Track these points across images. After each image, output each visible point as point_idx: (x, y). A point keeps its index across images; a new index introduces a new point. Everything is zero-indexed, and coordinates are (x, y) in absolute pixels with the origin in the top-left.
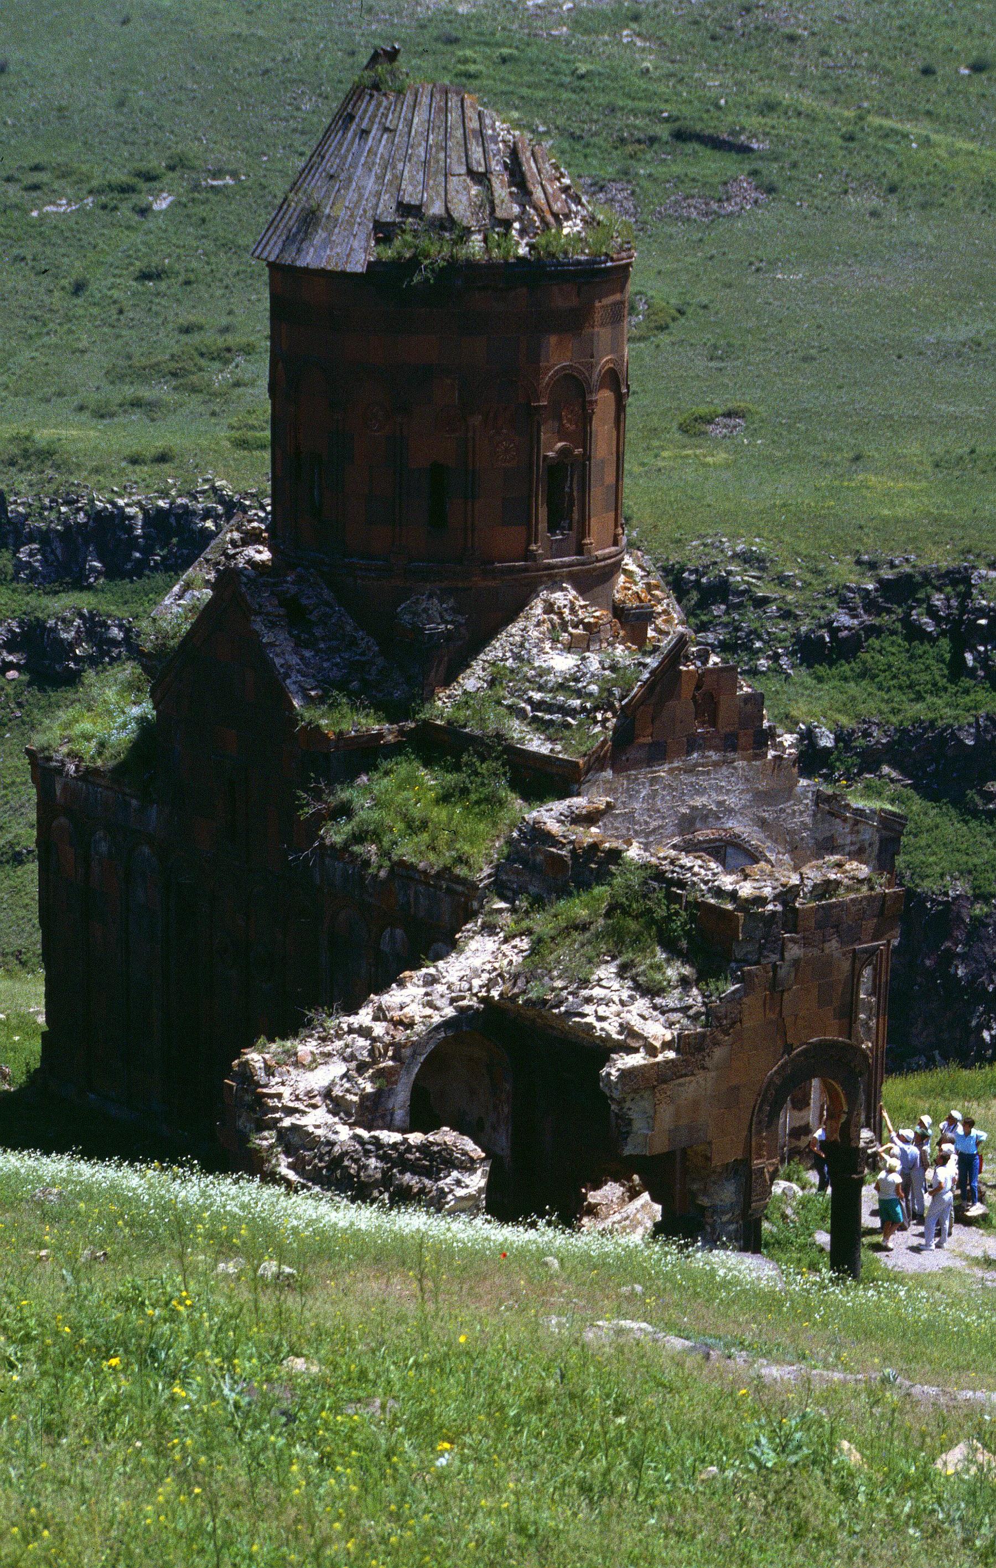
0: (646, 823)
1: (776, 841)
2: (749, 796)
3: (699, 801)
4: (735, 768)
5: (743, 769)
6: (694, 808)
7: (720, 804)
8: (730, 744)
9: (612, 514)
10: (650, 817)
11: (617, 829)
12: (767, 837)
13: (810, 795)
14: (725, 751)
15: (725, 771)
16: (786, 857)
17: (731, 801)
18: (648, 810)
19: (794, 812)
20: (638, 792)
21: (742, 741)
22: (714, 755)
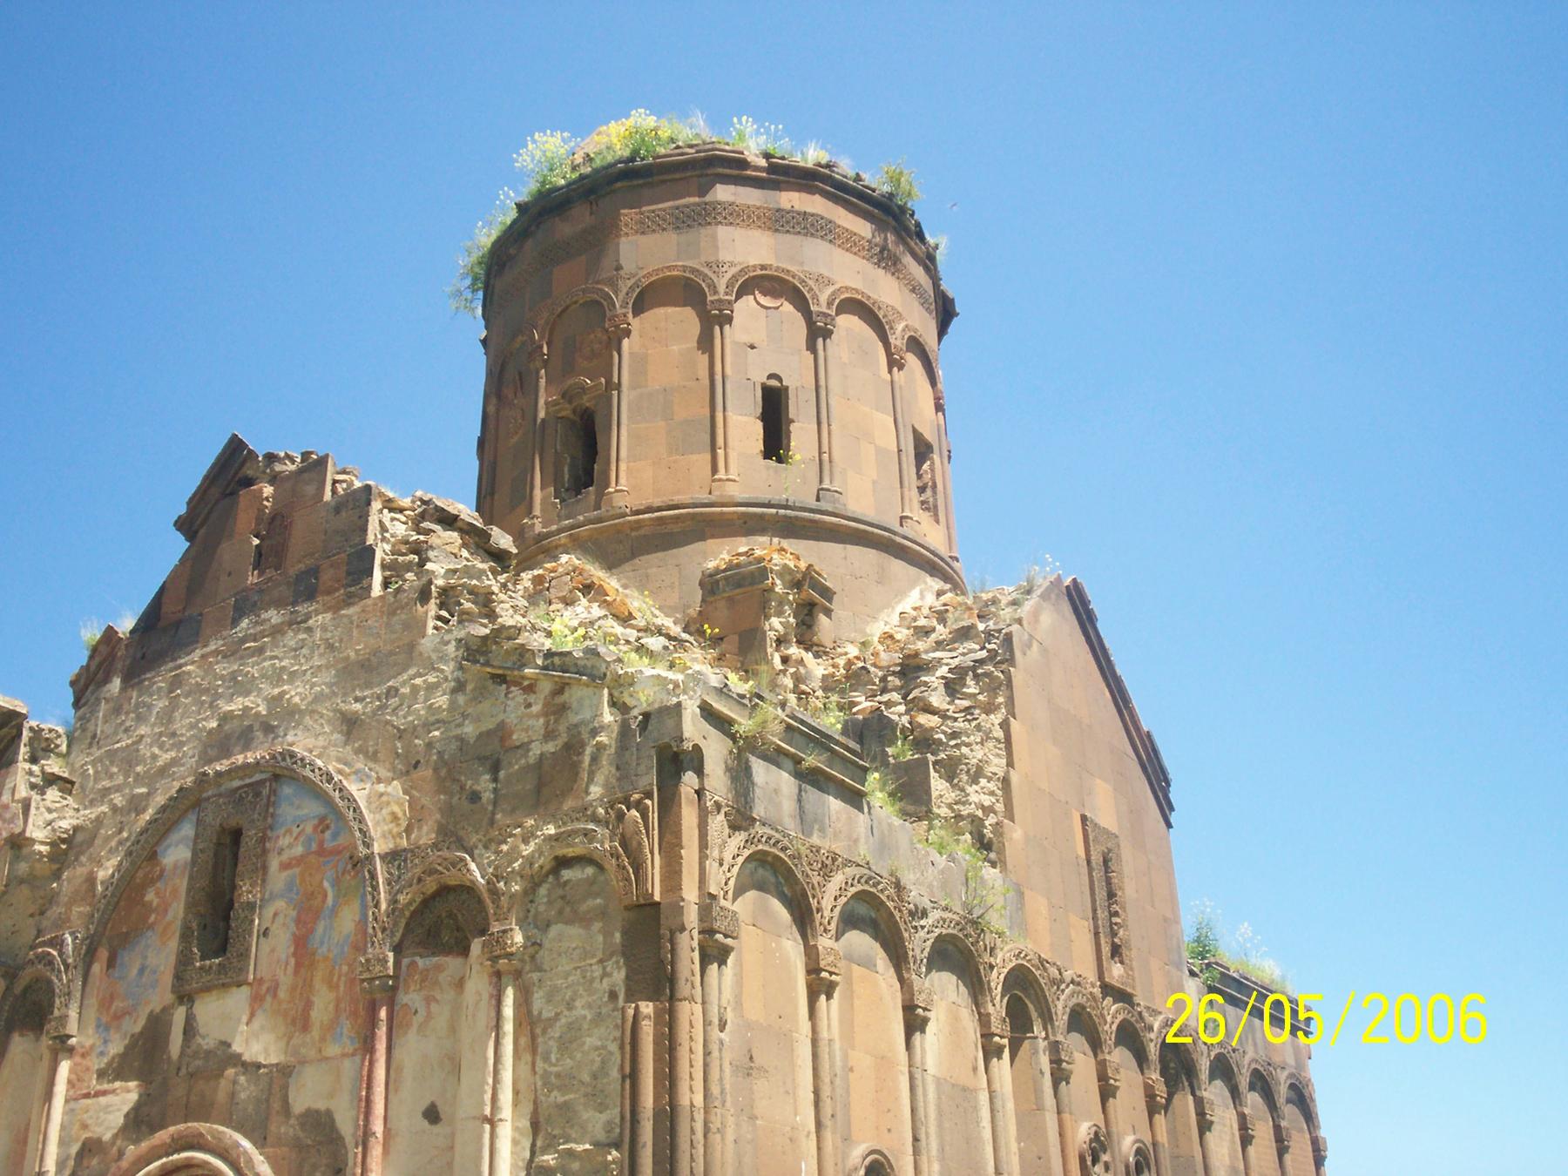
0: (154, 757)
1: (373, 757)
2: (328, 676)
3: (236, 705)
4: (309, 630)
5: (324, 629)
6: (225, 718)
7: (275, 701)
8: (306, 589)
9: (708, 457)
10: (161, 747)
11: (111, 776)
12: (357, 752)
13: (451, 648)
14: (294, 604)
15: (291, 639)
16: (396, 788)
17: (296, 693)
18: (161, 735)
19: (415, 689)
20: (150, 707)
21: (327, 576)
22: (274, 616)
